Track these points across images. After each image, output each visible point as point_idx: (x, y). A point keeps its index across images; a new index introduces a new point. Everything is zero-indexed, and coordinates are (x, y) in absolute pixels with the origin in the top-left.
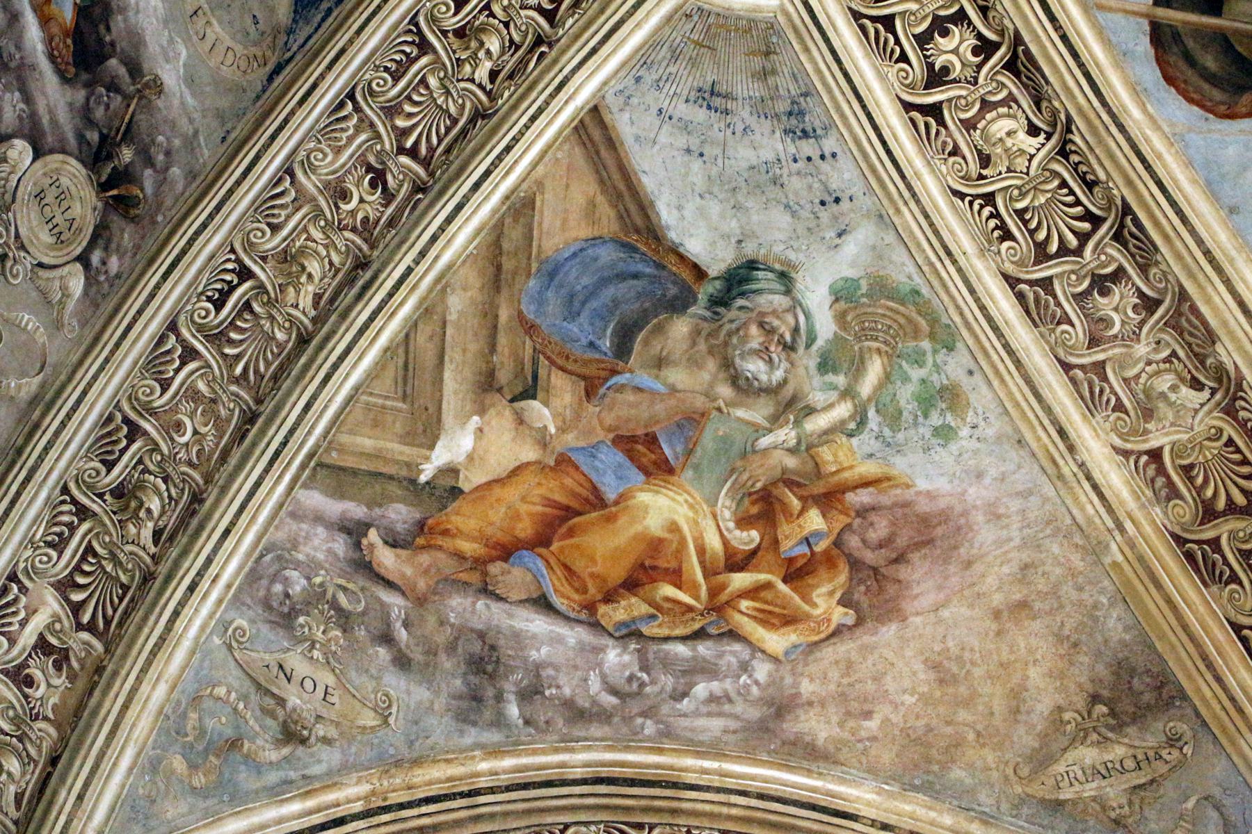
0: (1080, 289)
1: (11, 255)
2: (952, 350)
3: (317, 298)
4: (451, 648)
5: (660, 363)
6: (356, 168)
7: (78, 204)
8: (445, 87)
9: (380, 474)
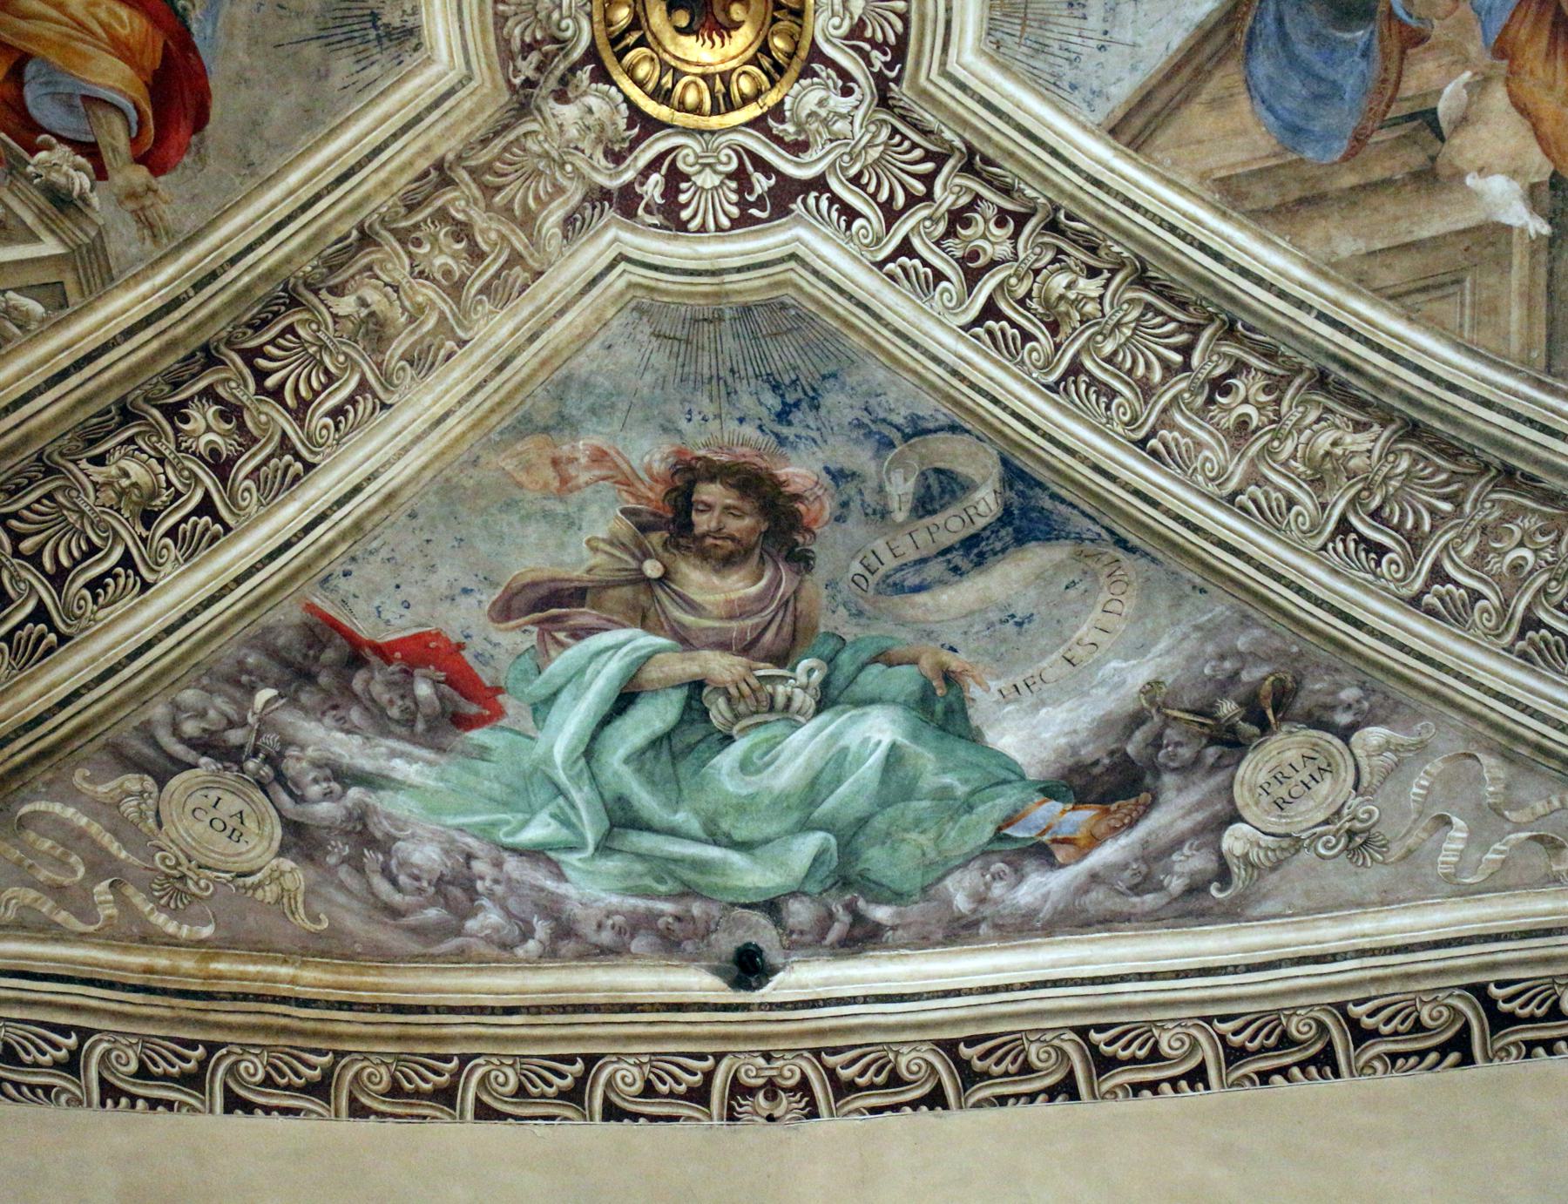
1: (1347, 825)
3: (1359, 427)
8: (1112, 331)
9: (1548, 287)
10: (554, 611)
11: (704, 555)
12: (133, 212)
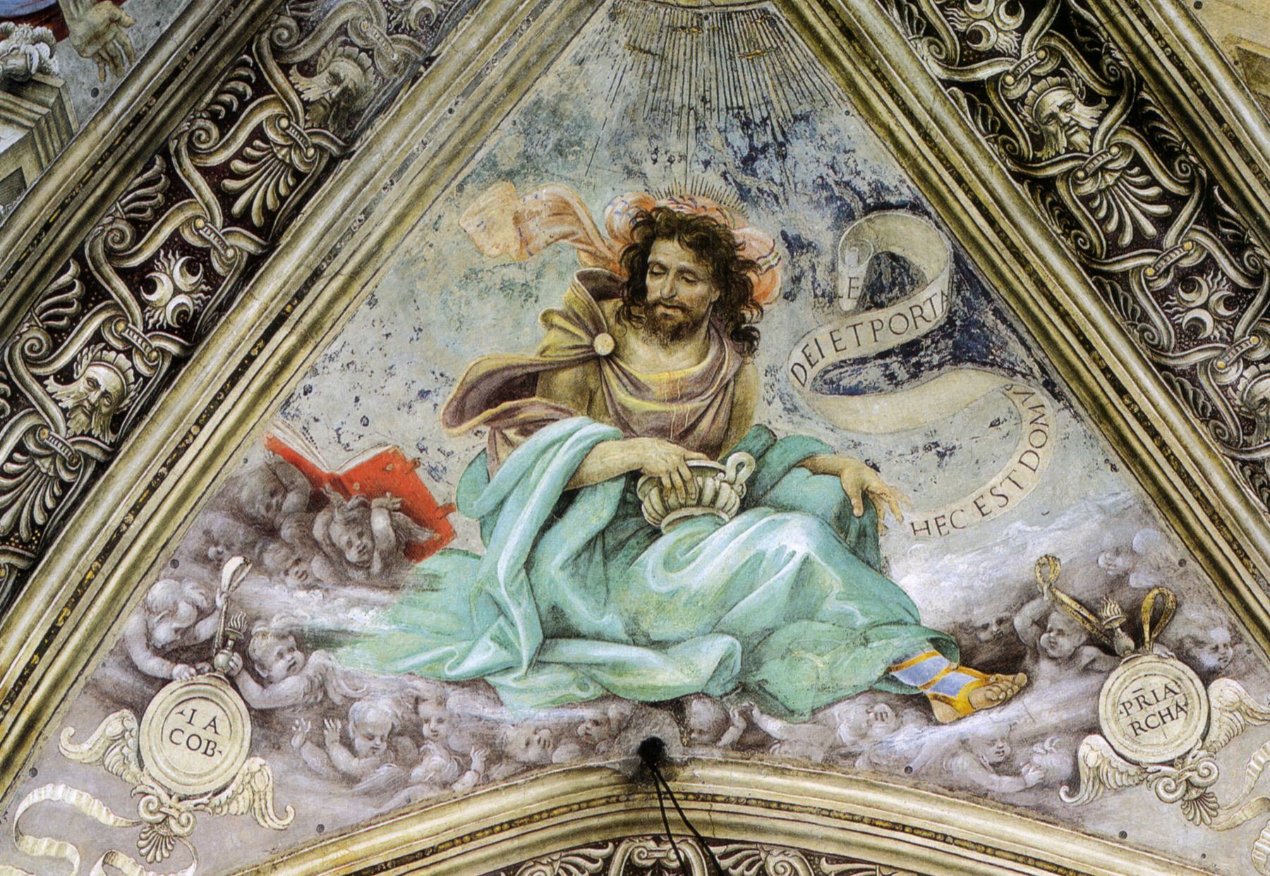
6: (1169, 307)
7: (1154, 680)
10: (506, 405)
11: (654, 327)
12: (93, 56)
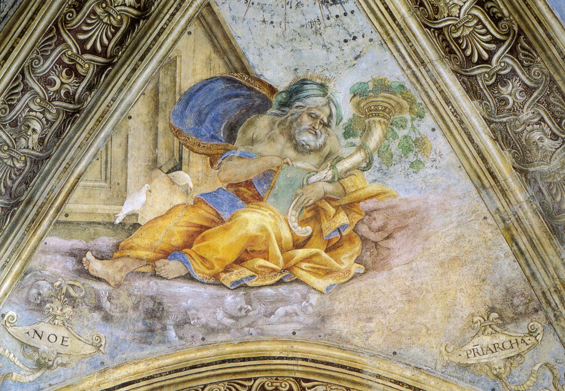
0: (491, 82)
2: (423, 117)
4: (136, 307)
5: (253, 141)
6: (56, 67)
